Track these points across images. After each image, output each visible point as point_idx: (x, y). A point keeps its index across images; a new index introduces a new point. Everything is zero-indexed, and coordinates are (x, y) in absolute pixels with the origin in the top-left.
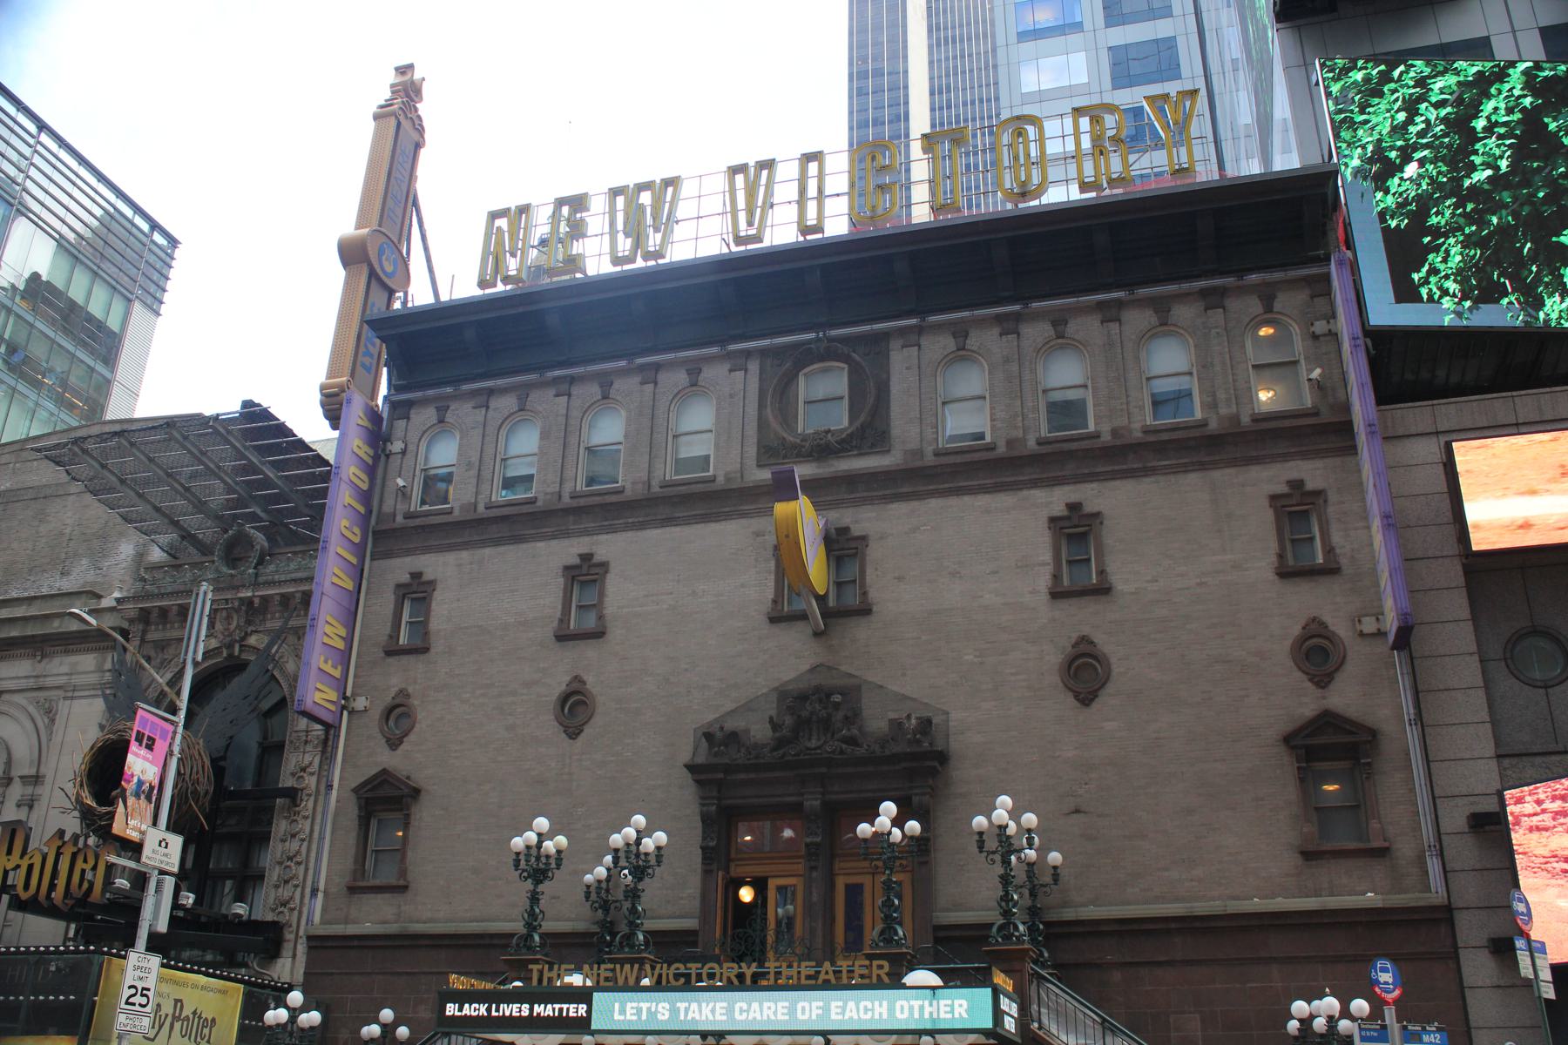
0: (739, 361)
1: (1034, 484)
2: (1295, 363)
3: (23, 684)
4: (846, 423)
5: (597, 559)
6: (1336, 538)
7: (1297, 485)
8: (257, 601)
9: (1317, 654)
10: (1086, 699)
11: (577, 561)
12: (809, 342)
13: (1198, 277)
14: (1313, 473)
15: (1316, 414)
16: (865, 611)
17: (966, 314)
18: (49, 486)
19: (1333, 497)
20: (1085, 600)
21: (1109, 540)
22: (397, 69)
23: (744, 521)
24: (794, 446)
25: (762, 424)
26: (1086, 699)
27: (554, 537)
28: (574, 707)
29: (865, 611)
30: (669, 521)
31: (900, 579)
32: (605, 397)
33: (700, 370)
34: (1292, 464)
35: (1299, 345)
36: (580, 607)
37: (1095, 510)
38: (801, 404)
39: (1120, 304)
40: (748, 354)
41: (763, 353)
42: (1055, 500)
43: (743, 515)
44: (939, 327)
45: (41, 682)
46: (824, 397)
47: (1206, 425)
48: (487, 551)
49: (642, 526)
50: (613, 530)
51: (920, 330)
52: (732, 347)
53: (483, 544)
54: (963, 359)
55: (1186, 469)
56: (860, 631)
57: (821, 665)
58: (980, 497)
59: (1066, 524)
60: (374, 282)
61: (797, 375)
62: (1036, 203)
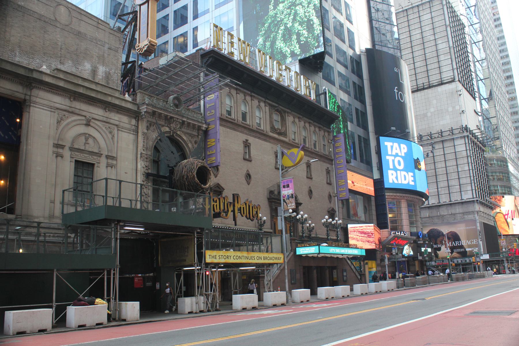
3: (101, 118)
5: (249, 142)
8: (186, 122)
9: (330, 197)
10: (311, 198)
18: (47, 18)
26: (311, 198)
28: (248, 176)
30: (259, 138)
35: (326, 143)
43: (270, 142)
45: (109, 120)
52: (267, 101)
53: (228, 127)
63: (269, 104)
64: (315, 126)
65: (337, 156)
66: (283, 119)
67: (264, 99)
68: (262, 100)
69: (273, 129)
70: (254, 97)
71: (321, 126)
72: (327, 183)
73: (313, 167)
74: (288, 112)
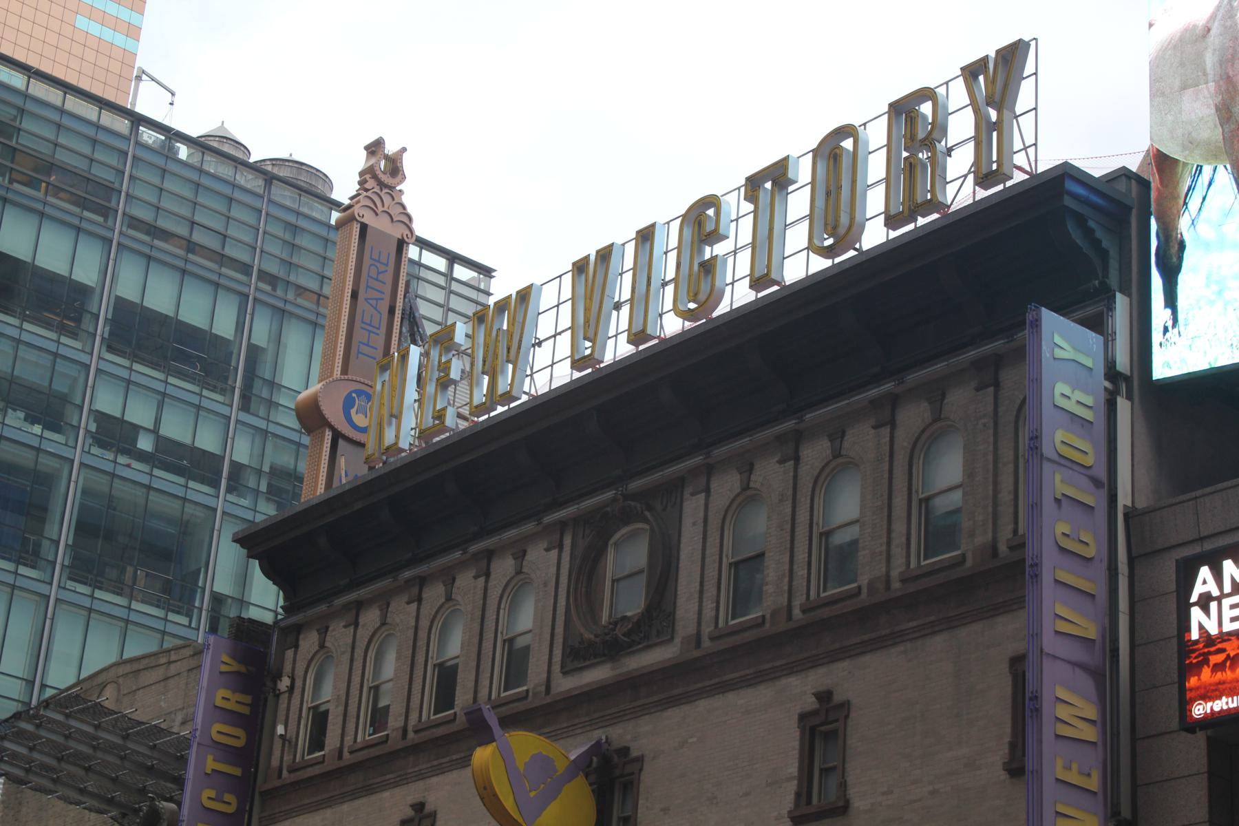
11: (410, 813)
17: (745, 440)
21: (853, 741)
22: (367, 148)
27: (396, 785)
31: (665, 810)
33: (524, 553)
36: (821, 770)
38: (608, 584)
40: (562, 525)
42: (801, 690)
48: (346, 807)
50: (440, 770)
52: (548, 519)
55: (930, 630)
60: (341, 442)
62: (852, 253)
67: (529, 527)
68: (532, 538)
71: (988, 348)
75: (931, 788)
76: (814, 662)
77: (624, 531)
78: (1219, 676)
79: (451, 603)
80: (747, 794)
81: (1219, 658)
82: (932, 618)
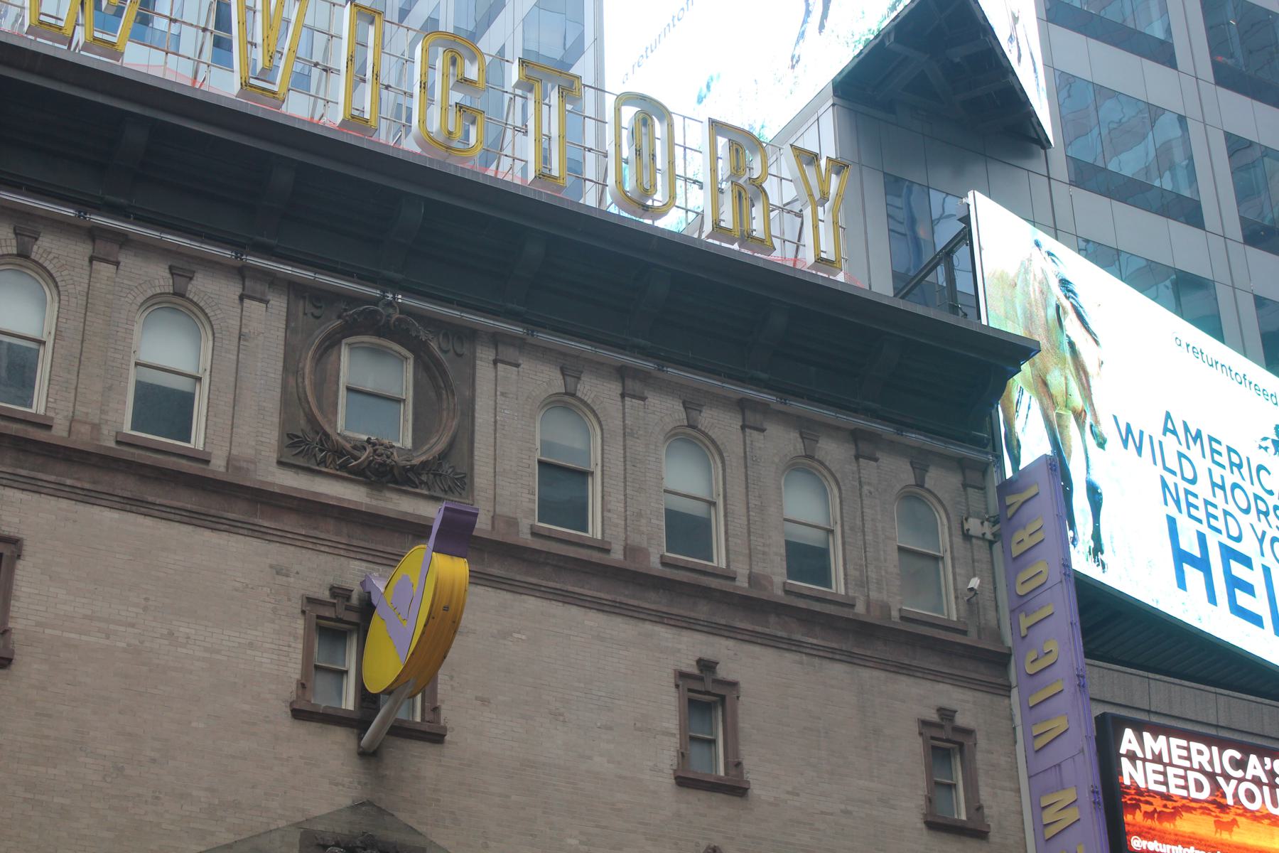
0: (253, 284)
1: (661, 618)
2: (936, 559)
4: (405, 439)
6: (985, 794)
7: (947, 714)
12: (375, 301)
13: (855, 411)
14: (968, 707)
15: (964, 633)
16: (436, 737)
19: (982, 742)
20: (717, 798)
21: (745, 724)
23: (256, 543)
24: (339, 452)
25: (291, 400)
29: (436, 737)
31: (484, 701)
32: (24, 255)
34: (941, 686)
35: (945, 540)
37: (731, 677)
39: (764, 409)
40: (273, 280)
41: (294, 289)
44: (544, 353)
46: (373, 389)
47: (853, 606)
49: (89, 497)
50: (32, 486)
51: (520, 344)
54: (566, 407)
55: (832, 655)
56: (422, 763)
57: (369, 803)
58: (593, 615)
59: (697, 686)
61: (338, 342)
63: (294, 289)
64: (808, 429)
65: (1025, 622)
66: (441, 389)
69: (308, 443)
70: (124, 241)
71: (877, 427)
72: (938, 825)
73: (753, 710)
74: (496, 339)
75: (843, 807)
76: (714, 629)
77: (374, 340)
78: (1149, 823)
79: (18, 261)
80: (610, 728)
81: (1149, 808)
82: (834, 645)
